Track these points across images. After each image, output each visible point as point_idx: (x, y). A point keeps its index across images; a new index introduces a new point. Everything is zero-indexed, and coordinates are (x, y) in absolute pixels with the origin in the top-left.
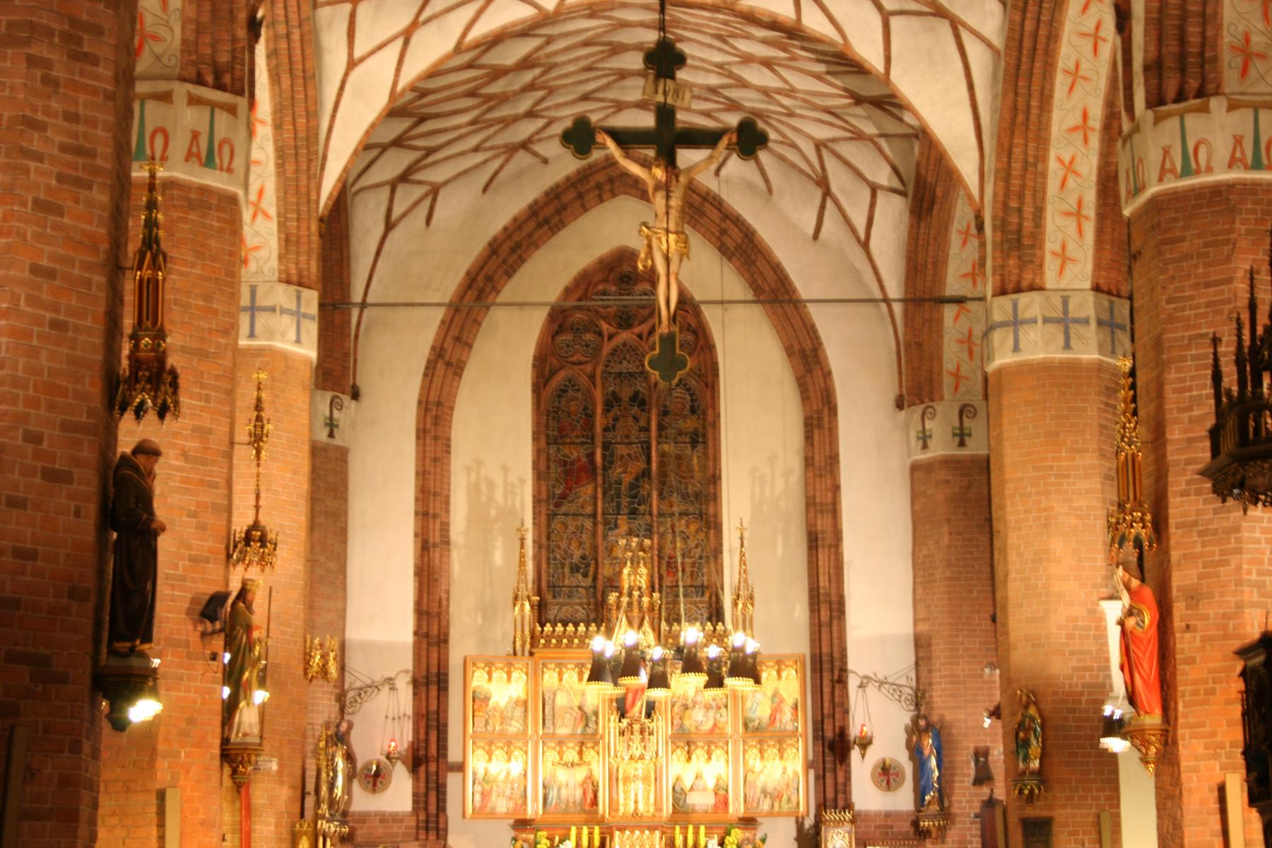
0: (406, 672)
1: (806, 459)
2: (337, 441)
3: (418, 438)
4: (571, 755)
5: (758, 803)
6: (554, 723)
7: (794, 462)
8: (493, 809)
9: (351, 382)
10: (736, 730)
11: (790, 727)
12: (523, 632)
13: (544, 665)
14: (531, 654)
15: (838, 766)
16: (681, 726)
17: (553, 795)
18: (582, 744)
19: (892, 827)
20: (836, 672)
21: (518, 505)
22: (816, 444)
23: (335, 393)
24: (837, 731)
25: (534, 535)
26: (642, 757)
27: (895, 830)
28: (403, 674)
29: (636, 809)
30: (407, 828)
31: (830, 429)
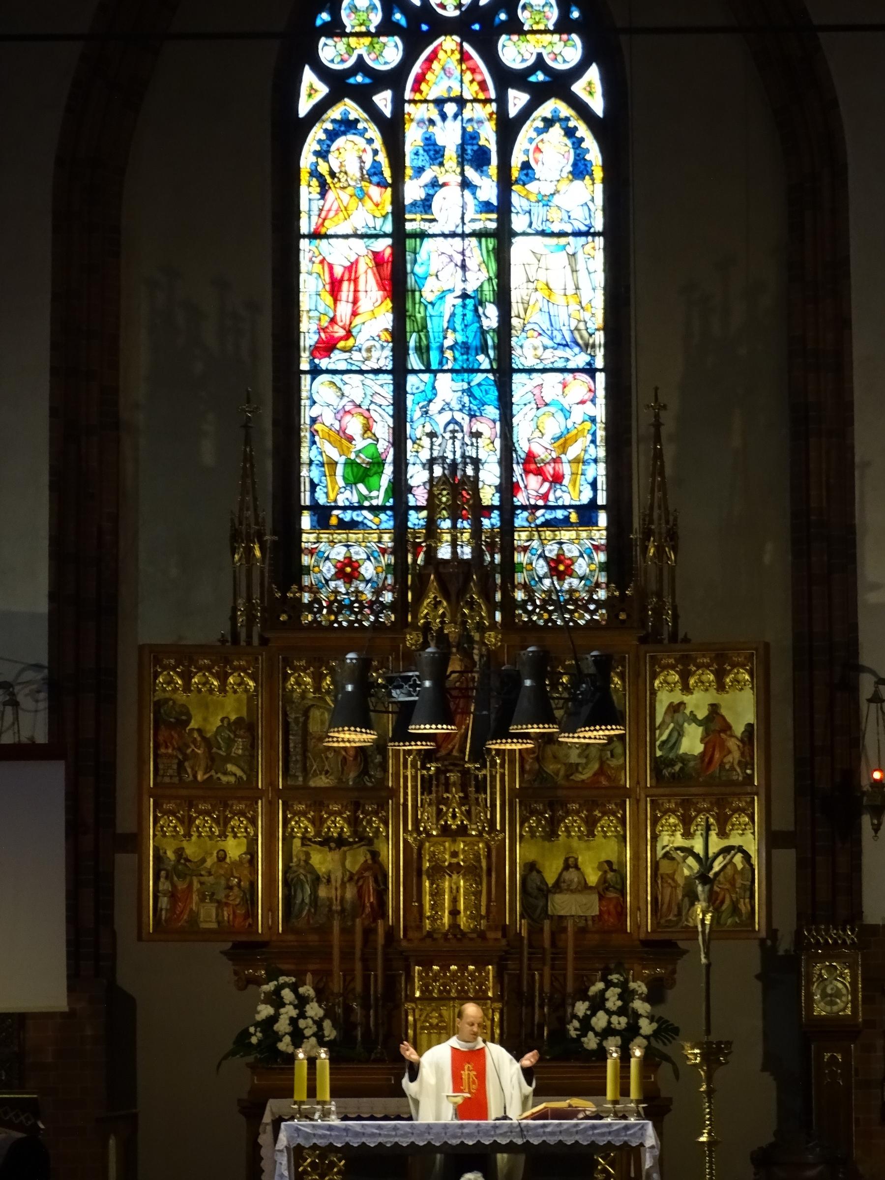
0: (38, 667)
4: (338, 825)
5: (679, 914)
6: (305, 770)
8: (194, 918)
10: (638, 781)
11: (738, 775)
12: (249, 599)
13: (287, 662)
14: (264, 641)
16: (541, 771)
18: (357, 806)
25: (275, 411)
26: (463, 831)
28: (29, 675)
29: (454, 925)
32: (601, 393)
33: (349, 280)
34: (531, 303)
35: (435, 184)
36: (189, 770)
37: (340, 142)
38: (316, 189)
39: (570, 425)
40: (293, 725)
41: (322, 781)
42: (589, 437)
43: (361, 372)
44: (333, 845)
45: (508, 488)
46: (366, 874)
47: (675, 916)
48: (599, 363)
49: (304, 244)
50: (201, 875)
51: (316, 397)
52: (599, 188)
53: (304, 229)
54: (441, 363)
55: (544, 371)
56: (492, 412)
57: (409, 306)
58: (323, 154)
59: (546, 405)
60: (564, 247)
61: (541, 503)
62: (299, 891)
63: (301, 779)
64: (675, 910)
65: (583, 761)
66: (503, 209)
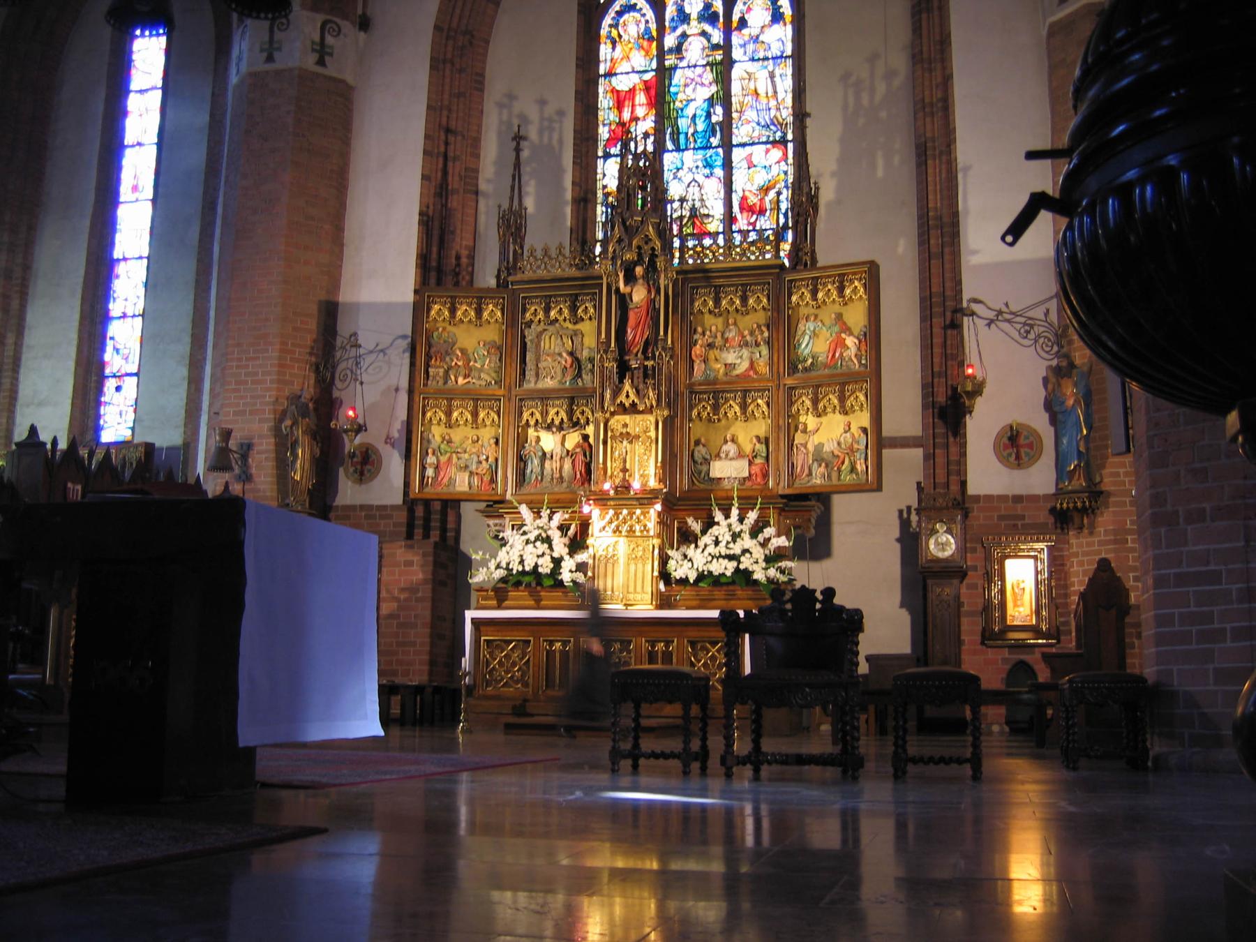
0: (404, 337)
1: (914, 56)
2: (331, 70)
3: (433, 67)
6: (537, 375)
7: (899, 61)
9: (360, 11)
15: (951, 439)
17: (533, 465)
19: (1023, 517)
20: (948, 314)
21: (555, 142)
22: (924, 32)
23: (329, 17)
24: (949, 392)
27: (1027, 521)
28: (400, 341)
30: (395, 525)
31: (940, 8)
33: (629, 99)
34: (745, 103)
35: (684, 36)
36: (453, 378)
37: (626, 16)
38: (610, 46)
40: (529, 344)
41: (548, 383)
42: (783, 184)
44: (554, 429)
45: (729, 219)
46: (578, 450)
47: (808, 476)
48: (790, 136)
50: (458, 452)
51: (606, 172)
52: (789, 28)
53: (602, 71)
54: (686, 144)
55: (753, 144)
56: (719, 172)
58: (615, 26)
59: (755, 166)
60: (766, 67)
61: (751, 228)
62: (530, 464)
63: (533, 382)
64: (806, 471)
65: (738, 361)
66: (727, 47)
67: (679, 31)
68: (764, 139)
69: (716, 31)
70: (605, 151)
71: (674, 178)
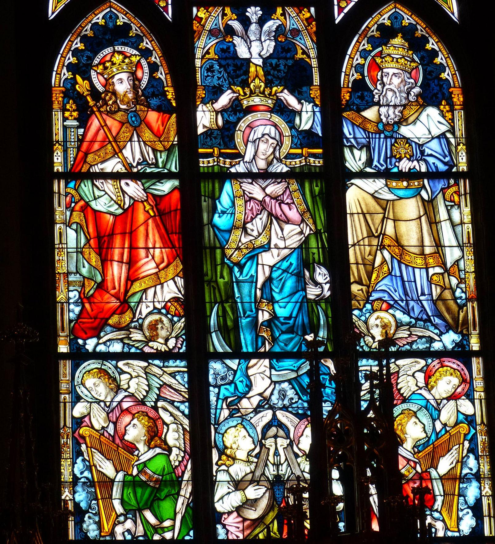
32: (479, 384)
39: (439, 426)
43: (142, 356)
48: (475, 344)
49: (59, 186)
51: (81, 390)
53: (58, 165)
57: (207, 267)
67: (224, 100)
68: (421, 346)
69: (308, 107)
70: (72, 343)
71: (231, 416)
